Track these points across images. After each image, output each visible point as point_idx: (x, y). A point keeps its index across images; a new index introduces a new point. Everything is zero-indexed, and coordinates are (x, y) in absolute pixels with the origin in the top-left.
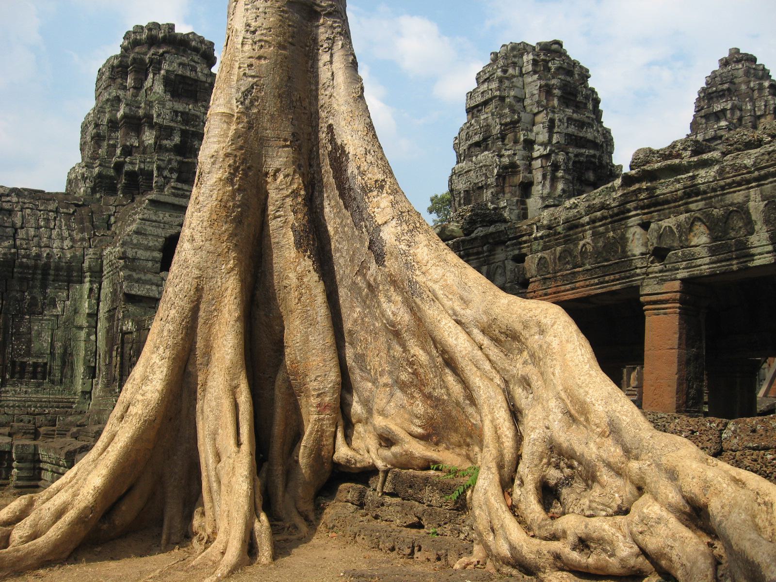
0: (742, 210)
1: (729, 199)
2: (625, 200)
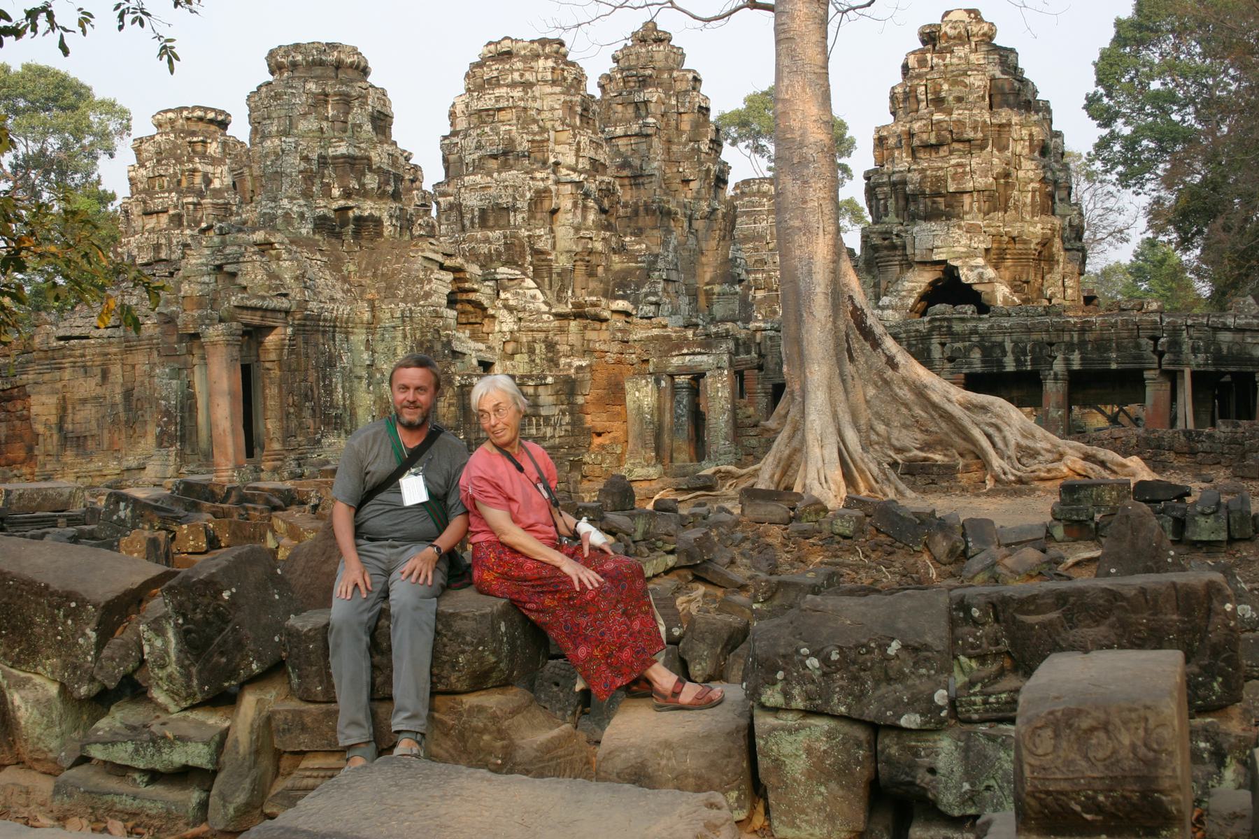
0: (1001, 345)
1: (993, 339)
2: (931, 330)
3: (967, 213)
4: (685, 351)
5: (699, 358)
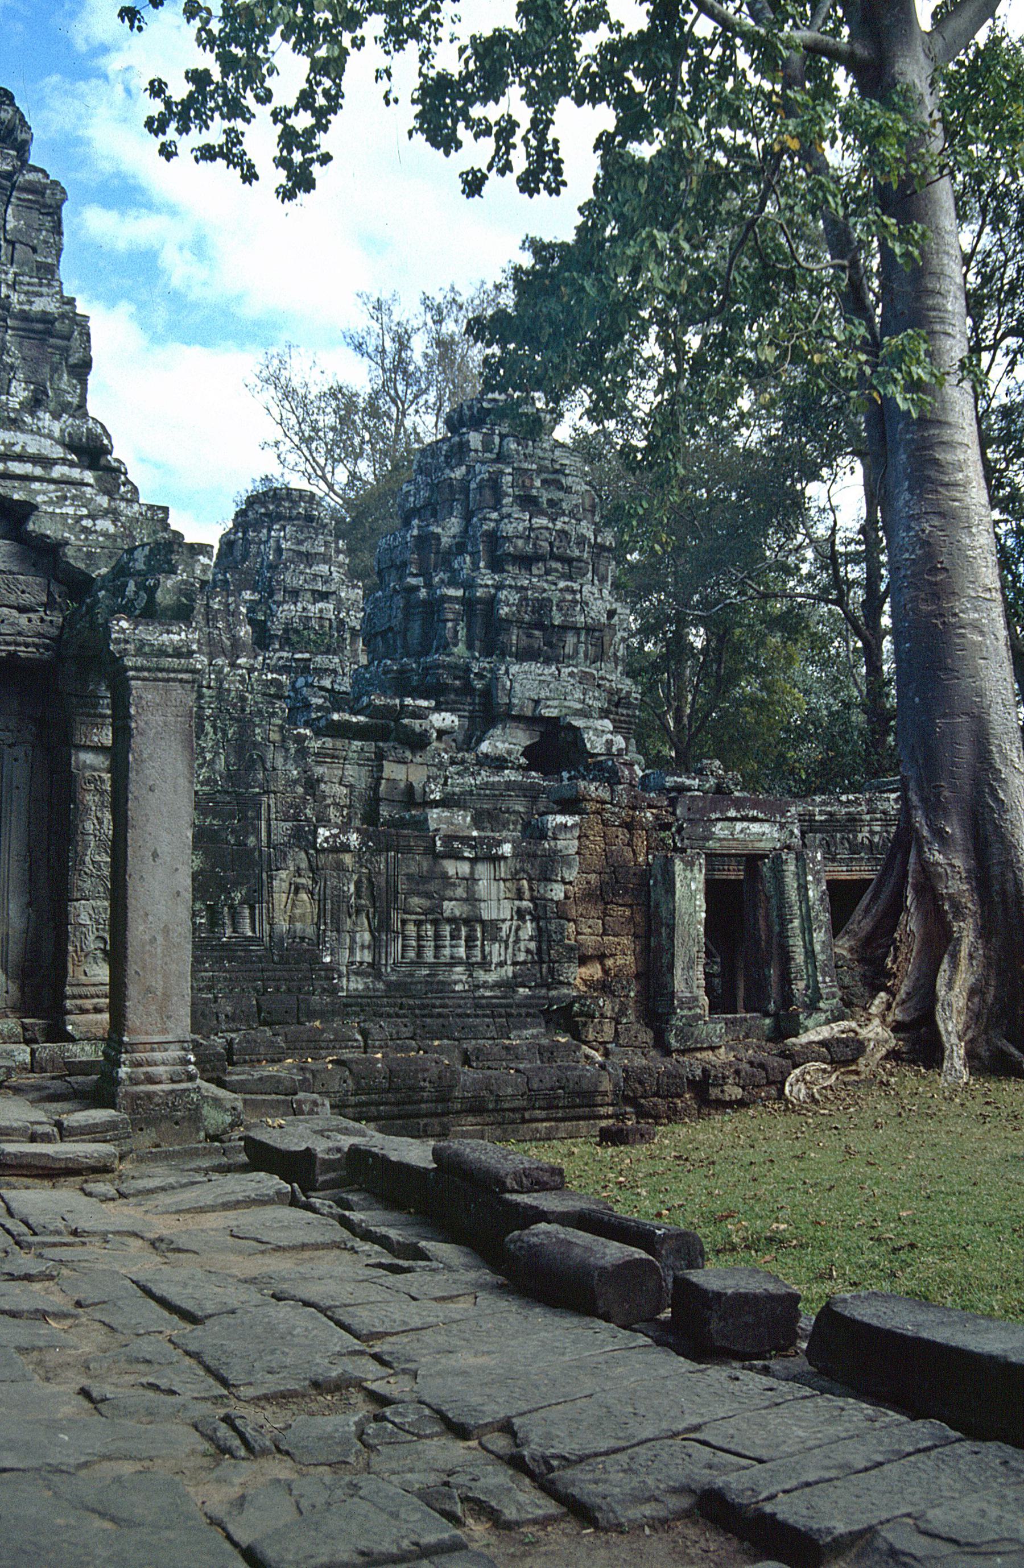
3: (569, 657)
4: (732, 813)
5: (755, 828)
